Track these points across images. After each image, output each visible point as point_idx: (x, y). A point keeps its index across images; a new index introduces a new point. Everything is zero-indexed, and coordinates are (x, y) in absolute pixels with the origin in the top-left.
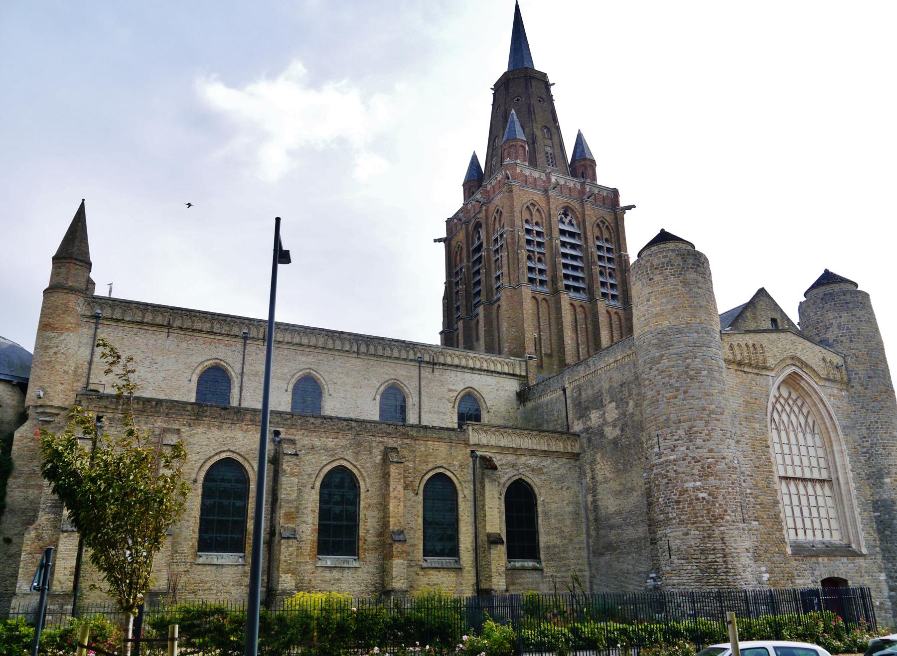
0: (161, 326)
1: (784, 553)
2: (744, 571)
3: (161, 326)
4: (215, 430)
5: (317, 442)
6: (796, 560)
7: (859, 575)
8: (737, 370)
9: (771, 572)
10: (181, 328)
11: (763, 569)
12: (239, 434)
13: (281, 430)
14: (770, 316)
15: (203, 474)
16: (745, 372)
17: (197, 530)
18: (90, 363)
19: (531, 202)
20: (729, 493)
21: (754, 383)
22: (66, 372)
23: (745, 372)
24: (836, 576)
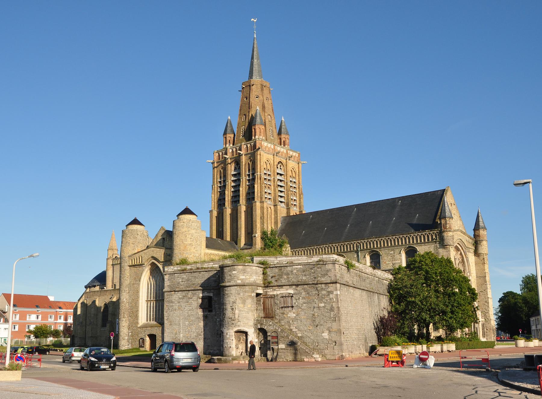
1: (137, 326)
9: (132, 332)
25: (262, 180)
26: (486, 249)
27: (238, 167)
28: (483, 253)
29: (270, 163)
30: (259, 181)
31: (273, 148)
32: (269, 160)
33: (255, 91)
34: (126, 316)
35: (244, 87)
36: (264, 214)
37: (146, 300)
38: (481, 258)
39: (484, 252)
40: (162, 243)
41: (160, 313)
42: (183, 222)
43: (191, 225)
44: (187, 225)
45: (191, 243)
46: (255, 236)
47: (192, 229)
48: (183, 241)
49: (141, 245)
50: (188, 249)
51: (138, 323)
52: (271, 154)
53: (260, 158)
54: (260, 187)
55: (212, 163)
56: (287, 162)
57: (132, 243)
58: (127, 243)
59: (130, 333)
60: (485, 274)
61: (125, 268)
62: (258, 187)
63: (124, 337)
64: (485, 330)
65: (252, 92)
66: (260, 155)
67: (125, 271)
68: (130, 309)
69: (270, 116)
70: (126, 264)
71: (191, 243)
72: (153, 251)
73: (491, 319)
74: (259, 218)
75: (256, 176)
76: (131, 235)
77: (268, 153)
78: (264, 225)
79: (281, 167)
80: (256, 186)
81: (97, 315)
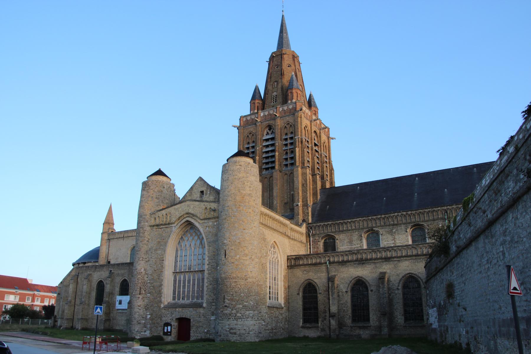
0: (122, 238)
1: (160, 307)
2: (135, 314)
3: (122, 238)
4: (98, 272)
5: (120, 272)
6: (164, 310)
7: (198, 316)
8: (156, 229)
9: (151, 315)
10: (126, 237)
11: (148, 313)
12: (103, 273)
13: (112, 270)
14: (200, 191)
15: (96, 286)
16: (161, 228)
17: (94, 302)
18: (108, 253)
19: (249, 133)
20: (136, 283)
21: (164, 232)
22: (103, 257)
23: (161, 228)
24: (184, 317)
27: (271, 132)
30: (300, 145)
33: (287, 60)
34: (144, 292)
35: (275, 56)
36: (307, 181)
37: (173, 271)
40: (200, 197)
41: (196, 289)
42: (240, 165)
43: (250, 170)
44: (244, 169)
45: (250, 192)
46: (298, 205)
47: (252, 175)
48: (239, 190)
49: (166, 201)
50: (247, 201)
51: (161, 302)
53: (301, 120)
54: (302, 151)
55: (238, 129)
56: (320, 133)
57: (156, 198)
58: (149, 197)
59: (148, 316)
61: (145, 229)
62: (299, 151)
63: (139, 320)
65: (284, 61)
66: (301, 117)
67: (145, 232)
68: (149, 282)
70: (147, 224)
71: (250, 193)
72: (188, 206)
74: (301, 185)
75: (297, 140)
76: (156, 188)
78: (307, 193)
79: (315, 138)
80: (297, 149)
81: (90, 293)
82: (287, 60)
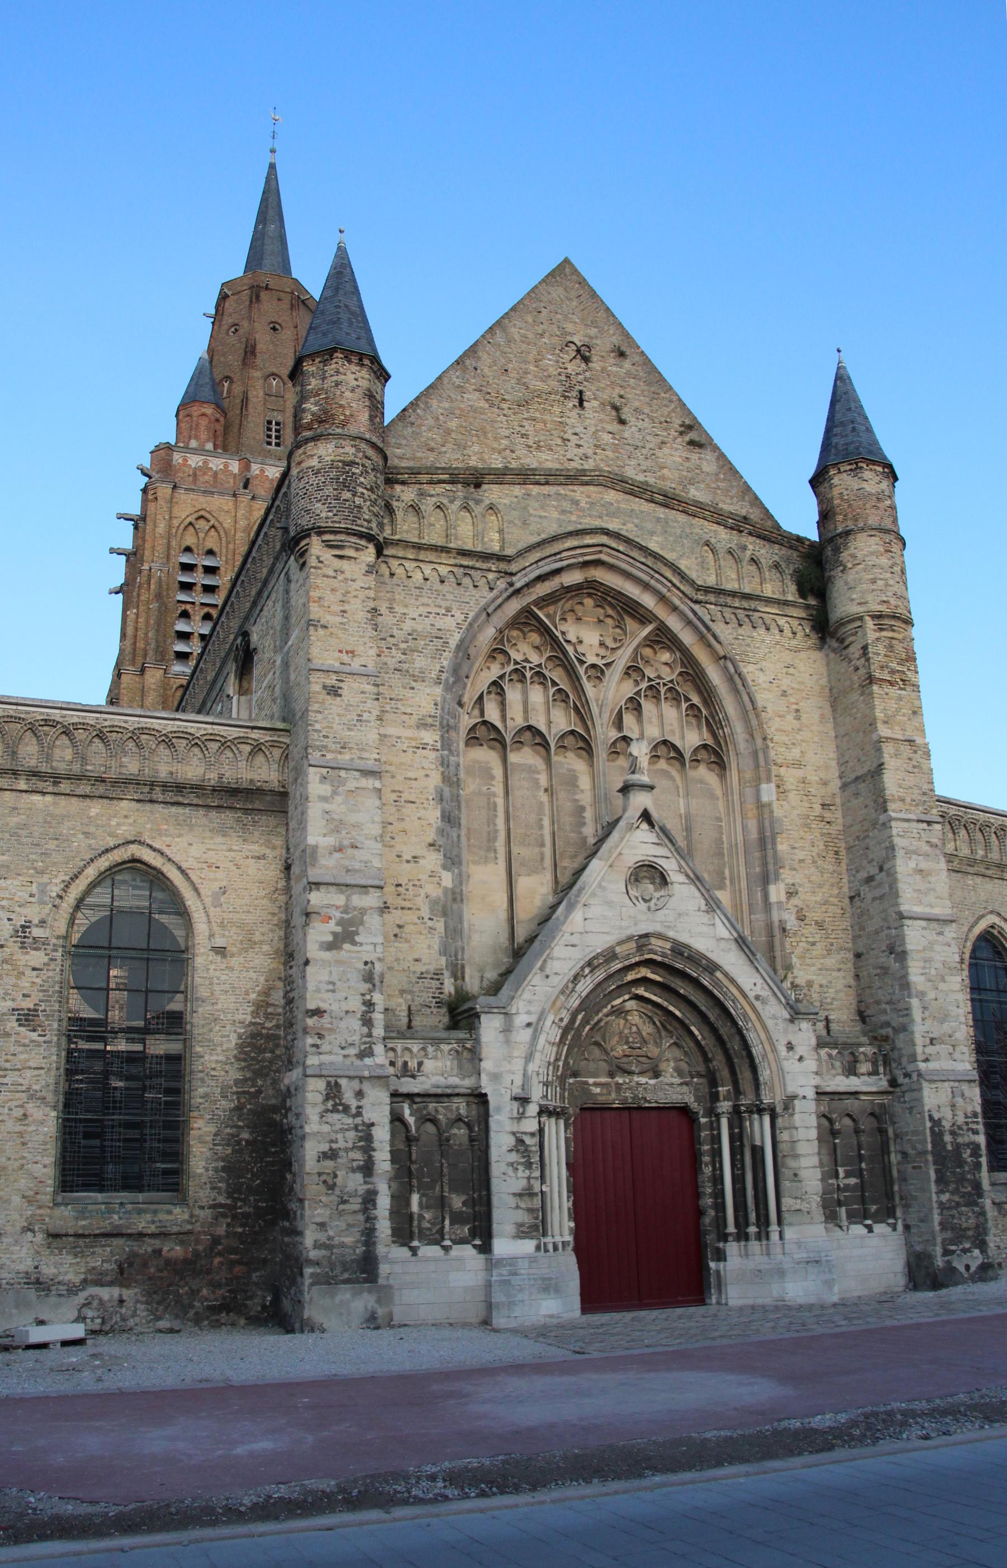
25: (153, 587)
26: (873, 581)
28: (854, 609)
29: (217, 524)
31: (236, 471)
32: (207, 515)
33: (230, 315)
38: (855, 651)
39: (860, 609)
52: (221, 494)
60: (879, 750)
62: (137, 618)
64: (894, 1158)
69: (279, 377)
73: (920, 1075)
77: (205, 492)
82: (230, 315)
